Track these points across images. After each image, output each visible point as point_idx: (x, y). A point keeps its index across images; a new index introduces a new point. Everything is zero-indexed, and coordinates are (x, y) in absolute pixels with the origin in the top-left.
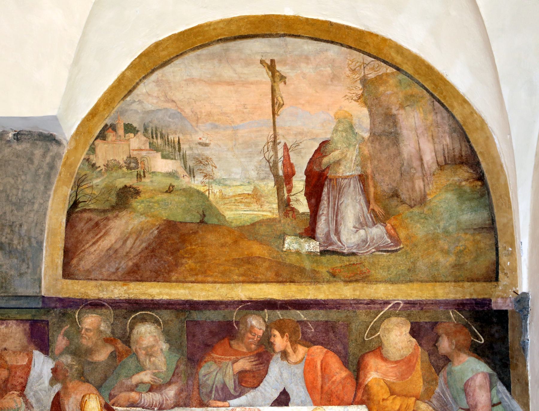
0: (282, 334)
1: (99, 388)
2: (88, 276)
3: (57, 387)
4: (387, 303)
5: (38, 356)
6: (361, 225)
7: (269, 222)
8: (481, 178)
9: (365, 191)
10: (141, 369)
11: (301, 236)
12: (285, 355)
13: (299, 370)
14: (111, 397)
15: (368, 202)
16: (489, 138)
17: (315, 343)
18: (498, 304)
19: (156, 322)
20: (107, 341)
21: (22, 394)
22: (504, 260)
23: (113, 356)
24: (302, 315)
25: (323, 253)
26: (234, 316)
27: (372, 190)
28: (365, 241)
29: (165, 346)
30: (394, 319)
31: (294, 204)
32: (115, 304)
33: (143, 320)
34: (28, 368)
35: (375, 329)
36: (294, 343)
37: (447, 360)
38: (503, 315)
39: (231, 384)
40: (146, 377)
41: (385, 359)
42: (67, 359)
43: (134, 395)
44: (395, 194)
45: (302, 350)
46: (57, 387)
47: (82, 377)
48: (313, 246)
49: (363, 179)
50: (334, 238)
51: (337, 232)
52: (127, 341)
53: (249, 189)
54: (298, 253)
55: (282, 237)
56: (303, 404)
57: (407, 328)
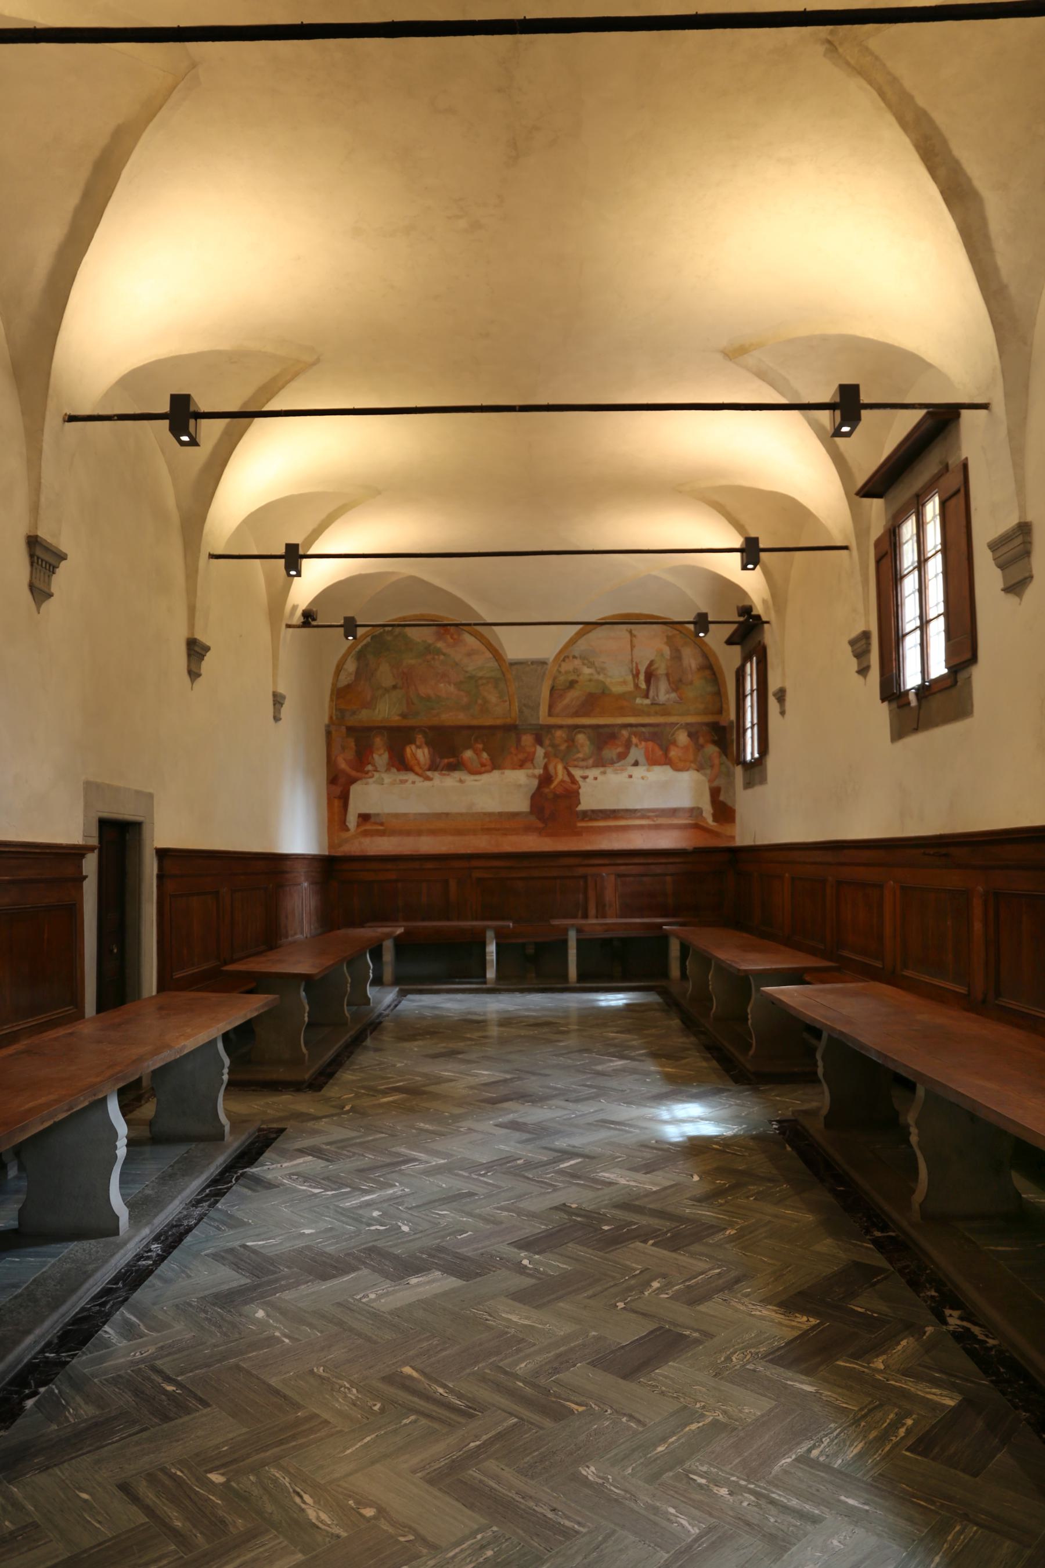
0: (635, 737)
1: (562, 760)
2: (557, 716)
3: (546, 760)
4: (678, 724)
5: (539, 748)
6: (667, 692)
7: (630, 693)
8: (714, 674)
9: (668, 680)
10: (579, 752)
11: (643, 697)
12: (636, 746)
13: (643, 751)
14: (567, 763)
15: (669, 684)
16: (717, 659)
17: (649, 740)
18: (723, 723)
19: (584, 733)
20: (566, 741)
21: (532, 763)
22: (724, 706)
23: (568, 747)
24: (643, 729)
25: (652, 704)
26: (616, 730)
27: (671, 679)
28: (668, 699)
29: (588, 743)
30: (681, 731)
31: (640, 685)
32: (569, 727)
33: (580, 732)
34: (534, 753)
35: (673, 734)
36: (640, 741)
37: (702, 746)
38: (724, 728)
39: (615, 757)
40: (580, 755)
41: (677, 746)
42: (550, 749)
43: (576, 763)
44: (680, 681)
45: (643, 743)
46: (546, 760)
47: (556, 756)
48: (647, 702)
49: (667, 675)
50: (656, 698)
51: (657, 696)
52: (573, 741)
53: (621, 680)
54: (642, 705)
55: (635, 698)
56: (644, 765)
57: (686, 734)
